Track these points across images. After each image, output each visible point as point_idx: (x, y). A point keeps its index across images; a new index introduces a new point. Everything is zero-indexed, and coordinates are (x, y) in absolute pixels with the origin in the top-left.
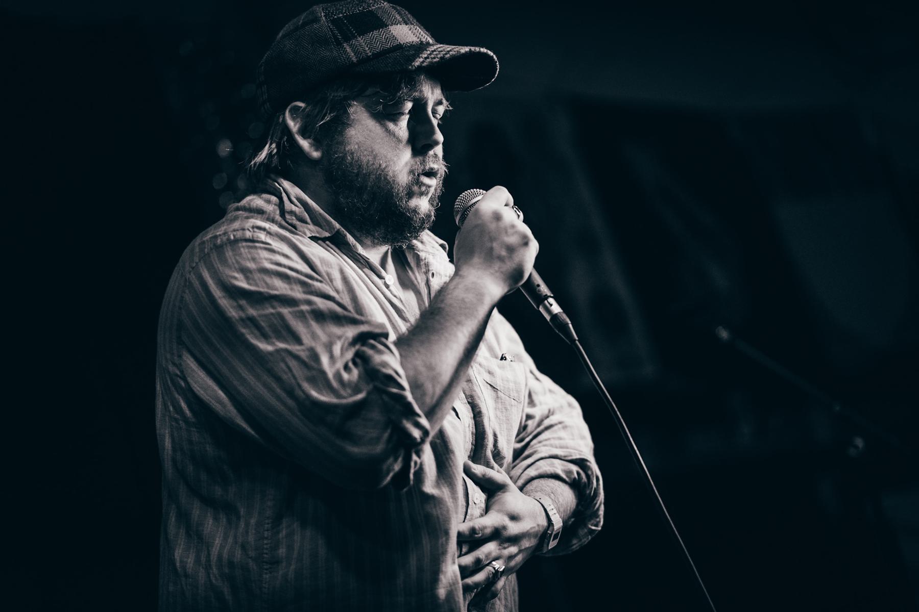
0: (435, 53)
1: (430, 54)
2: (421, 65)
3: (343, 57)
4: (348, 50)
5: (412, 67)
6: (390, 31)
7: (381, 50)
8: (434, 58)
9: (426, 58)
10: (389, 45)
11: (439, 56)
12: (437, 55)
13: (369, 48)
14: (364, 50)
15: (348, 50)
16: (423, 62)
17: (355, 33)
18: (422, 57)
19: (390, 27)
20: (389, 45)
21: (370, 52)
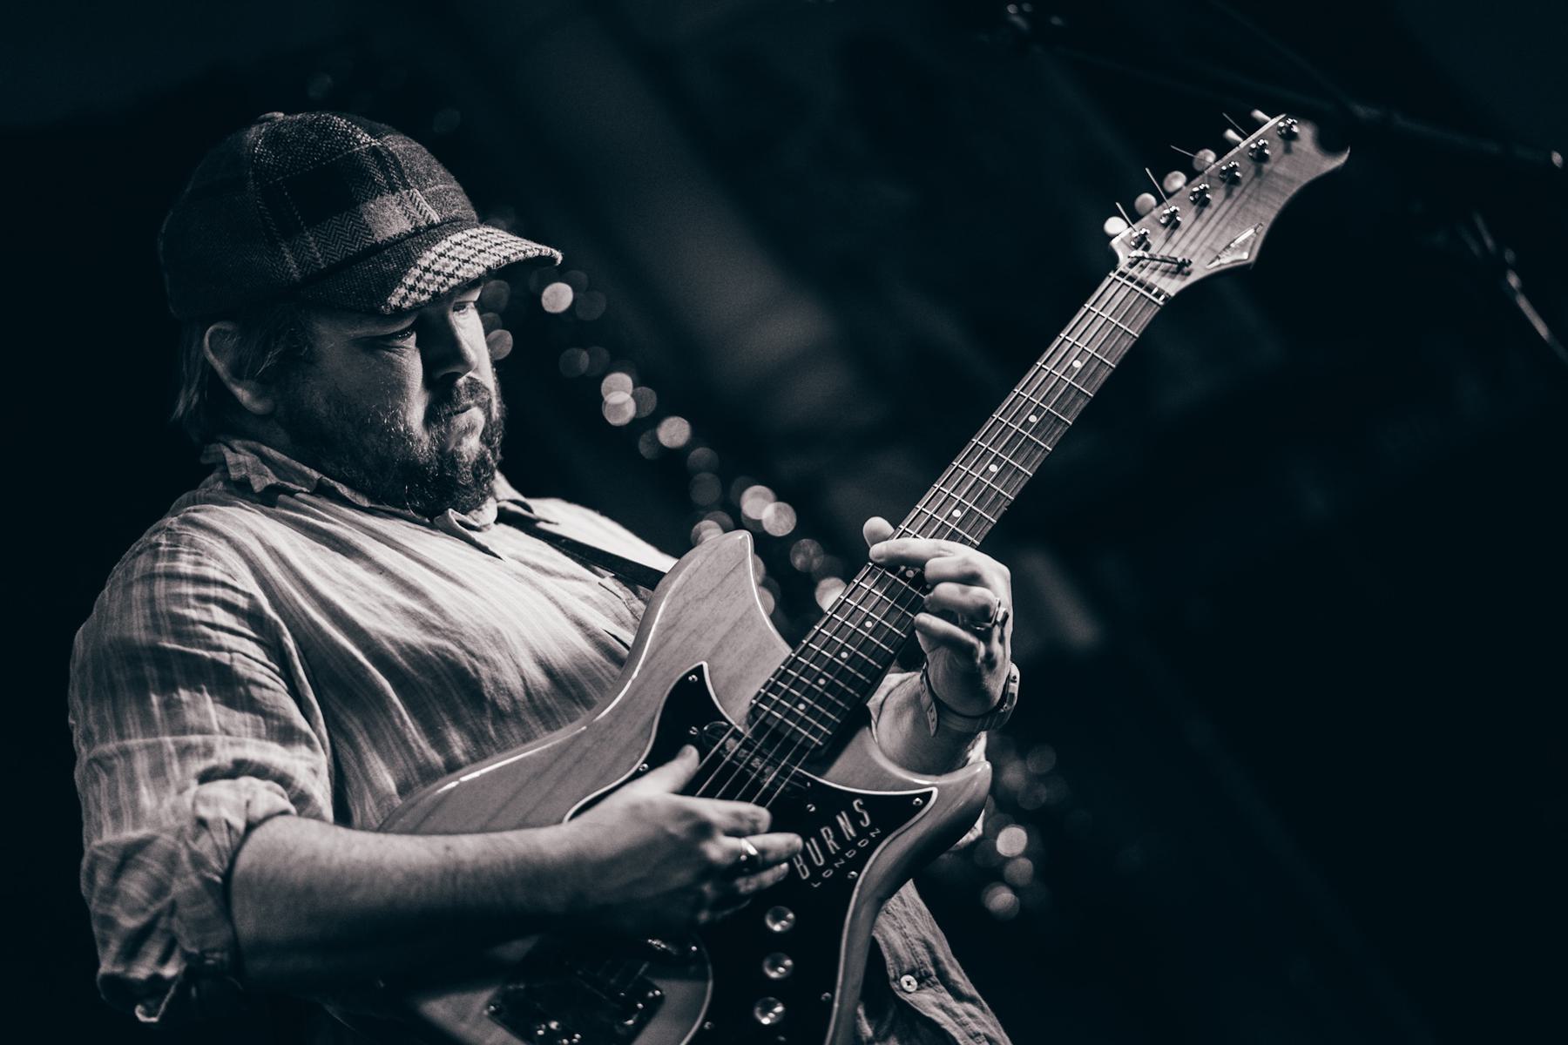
0: (429, 276)
1: (419, 279)
2: (401, 305)
3: (279, 270)
4: (289, 257)
5: (386, 308)
6: (361, 215)
7: (343, 257)
8: (423, 292)
9: (412, 288)
10: (357, 246)
11: (432, 288)
12: (430, 282)
13: (323, 255)
14: (314, 258)
15: (289, 257)
16: (405, 298)
17: (301, 220)
18: (405, 284)
19: (360, 206)
20: (357, 246)
21: (325, 262)
